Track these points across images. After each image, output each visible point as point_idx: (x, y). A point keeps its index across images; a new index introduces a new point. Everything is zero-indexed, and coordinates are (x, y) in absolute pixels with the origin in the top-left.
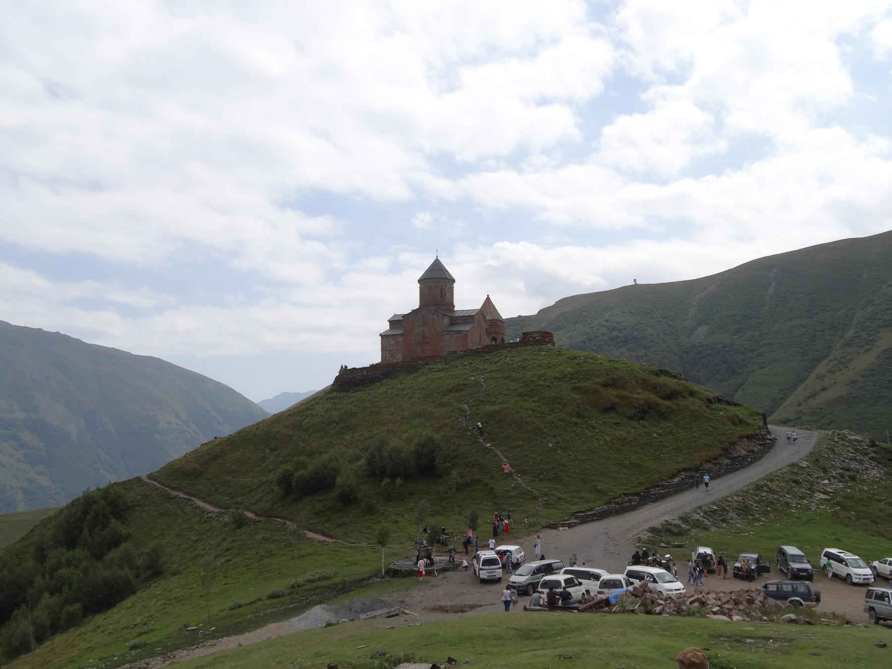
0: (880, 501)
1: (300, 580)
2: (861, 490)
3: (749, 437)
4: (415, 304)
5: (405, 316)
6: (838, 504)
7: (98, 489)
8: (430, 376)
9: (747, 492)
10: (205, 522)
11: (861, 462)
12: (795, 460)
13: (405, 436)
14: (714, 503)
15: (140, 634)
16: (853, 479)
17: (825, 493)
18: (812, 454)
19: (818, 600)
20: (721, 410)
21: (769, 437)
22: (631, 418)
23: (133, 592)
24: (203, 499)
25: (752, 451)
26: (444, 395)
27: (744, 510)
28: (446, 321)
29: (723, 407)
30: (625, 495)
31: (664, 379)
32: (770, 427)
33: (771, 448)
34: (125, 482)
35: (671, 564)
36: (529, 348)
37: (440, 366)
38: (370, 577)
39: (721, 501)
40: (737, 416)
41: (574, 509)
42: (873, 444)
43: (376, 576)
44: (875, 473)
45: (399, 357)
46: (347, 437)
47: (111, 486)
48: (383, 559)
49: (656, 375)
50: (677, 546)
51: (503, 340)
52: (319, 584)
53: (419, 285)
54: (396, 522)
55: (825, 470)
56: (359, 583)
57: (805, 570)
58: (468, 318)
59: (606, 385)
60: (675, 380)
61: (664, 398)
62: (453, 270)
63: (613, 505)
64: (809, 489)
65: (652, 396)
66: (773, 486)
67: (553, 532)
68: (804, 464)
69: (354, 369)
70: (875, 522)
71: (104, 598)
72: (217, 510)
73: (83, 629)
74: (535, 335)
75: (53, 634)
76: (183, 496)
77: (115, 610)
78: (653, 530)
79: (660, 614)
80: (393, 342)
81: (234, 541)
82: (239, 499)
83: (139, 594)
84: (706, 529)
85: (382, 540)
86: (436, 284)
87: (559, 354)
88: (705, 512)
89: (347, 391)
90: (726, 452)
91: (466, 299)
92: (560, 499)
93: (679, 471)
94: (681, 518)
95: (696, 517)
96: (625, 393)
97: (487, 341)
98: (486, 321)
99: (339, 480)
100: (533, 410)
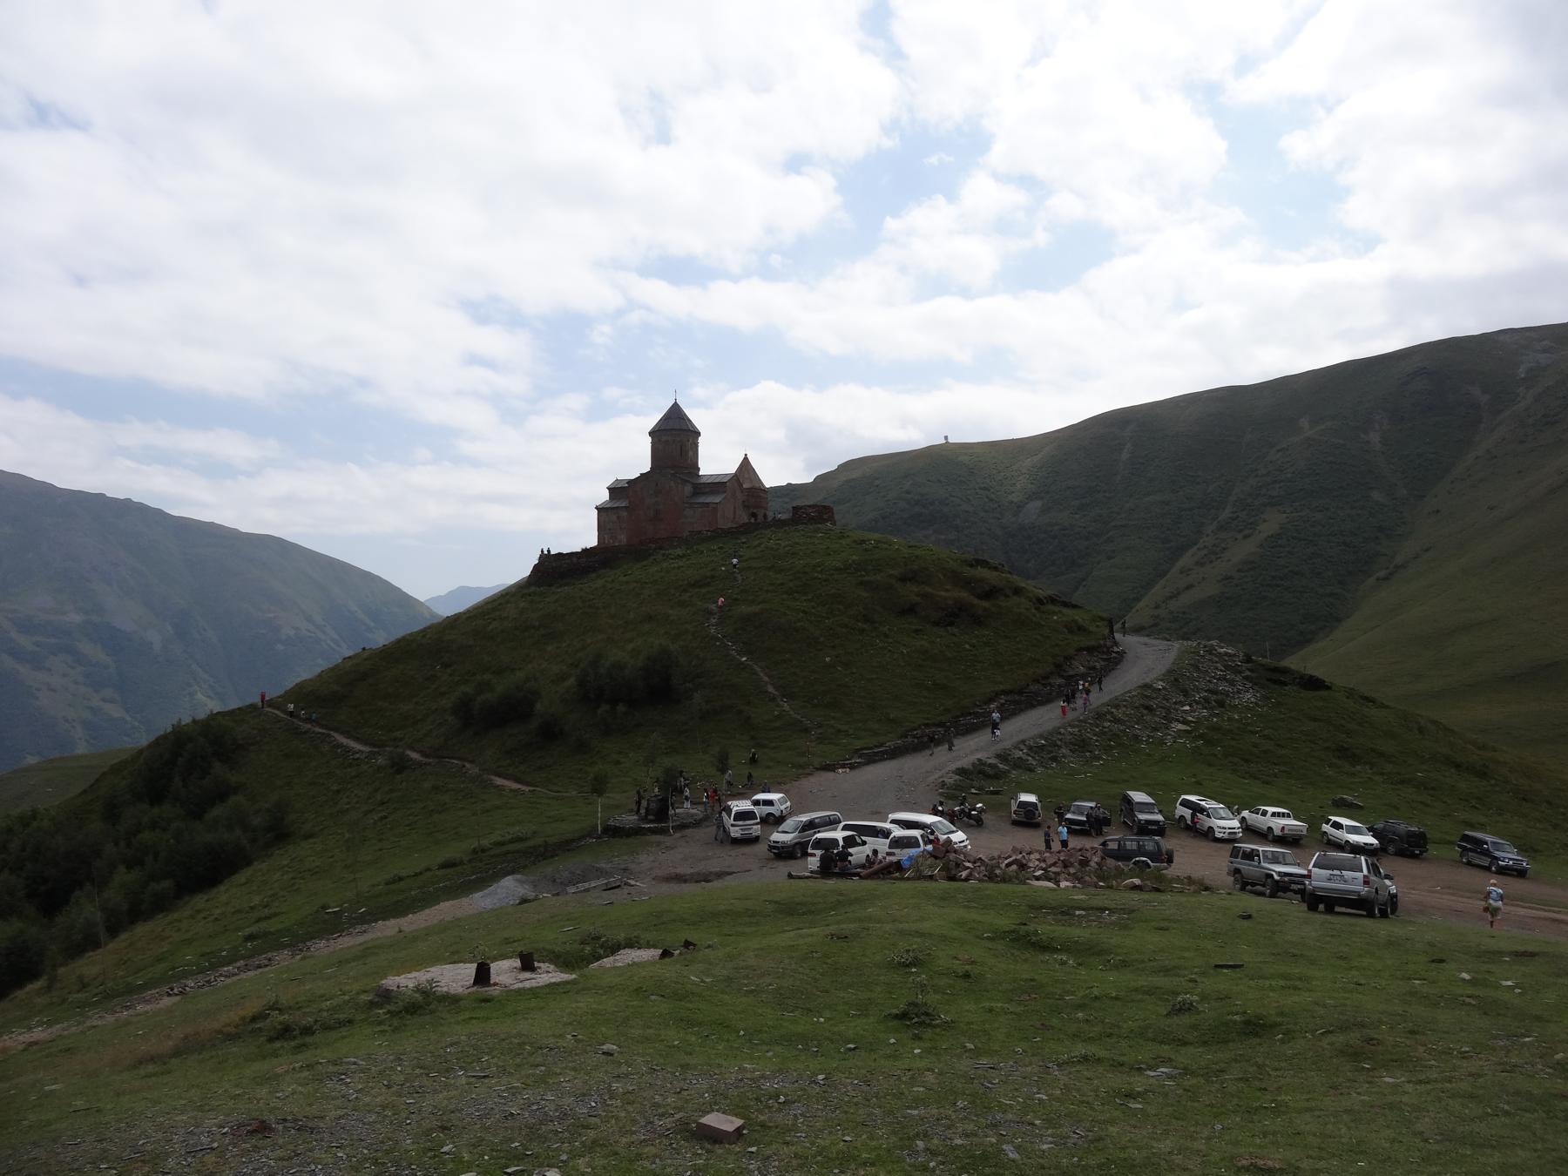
0: (1254, 733)
1: (485, 842)
2: (1230, 719)
3: (1090, 650)
4: (645, 465)
5: (630, 482)
6: (1201, 737)
7: (194, 721)
8: (665, 565)
10: (350, 765)
11: (1232, 683)
12: (1148, 680)
13: (630, 647)
14: (1041, 736)
15: (259, 920)
16: (1221, 704)
17: (1185, 722)
18: (1170, 672)
19: (1170, 860)
20: (1054, 613)
22: (936, 624)
23: (249, 863)
24: (348, 735)
25: (1094, 668)
26: (685, 591)
27: (1080, 745)
28: (688, 489)
29: (1056, 609)
30: (927, 725)
31: (981, 572)
32: (1118, 636)
33: (1117, 664)
34: (232, 712)
35: (984, 816)
36: (801, 527)
37: (679, 552)
40: (1075, 621)
41: (858, 744)
42: (1248, 660)
43: (590, 835)
44: (1249, 696)
45: (623, 539)
47: (213, 716)
48: (599, 812)
50: (993, 793)
51: (765, 516)
52: (511, 847)
54: (618, 763)
55: (1185, 693)
56: (568, 846)
57: (1156, 822)
58: (718, 485)
59: (903, 579)
60: (995, 573)
61: (980, 597)
62: (696, 416)
63: (910, 739)
65: (964, 595)
66: (1119, 714)
67: (830, 775)
68: (1160, 685)
69: (560, 554)
70: (1247, 761)
71: (206, 871)
72: (366, 749)
73: (176, 916)
74: (809, 509)
75: (132, 923)
77: (222, 888)
78: (961, 771)
79: (966, 880)
80: (614, 518)
82: (398, 734)
83: (257, 865)
84: (1031, 770)
85: (599, 786)
86: (675, 437)
88: (1030, 748)
89: (550, 585)
90: (1059, 668)
91: (715, 460)
94: (998, 756)
95: (1019, 754)
96: (929, 590)
97: (744, 518)
98: (742, 490)
99: (539, 707)
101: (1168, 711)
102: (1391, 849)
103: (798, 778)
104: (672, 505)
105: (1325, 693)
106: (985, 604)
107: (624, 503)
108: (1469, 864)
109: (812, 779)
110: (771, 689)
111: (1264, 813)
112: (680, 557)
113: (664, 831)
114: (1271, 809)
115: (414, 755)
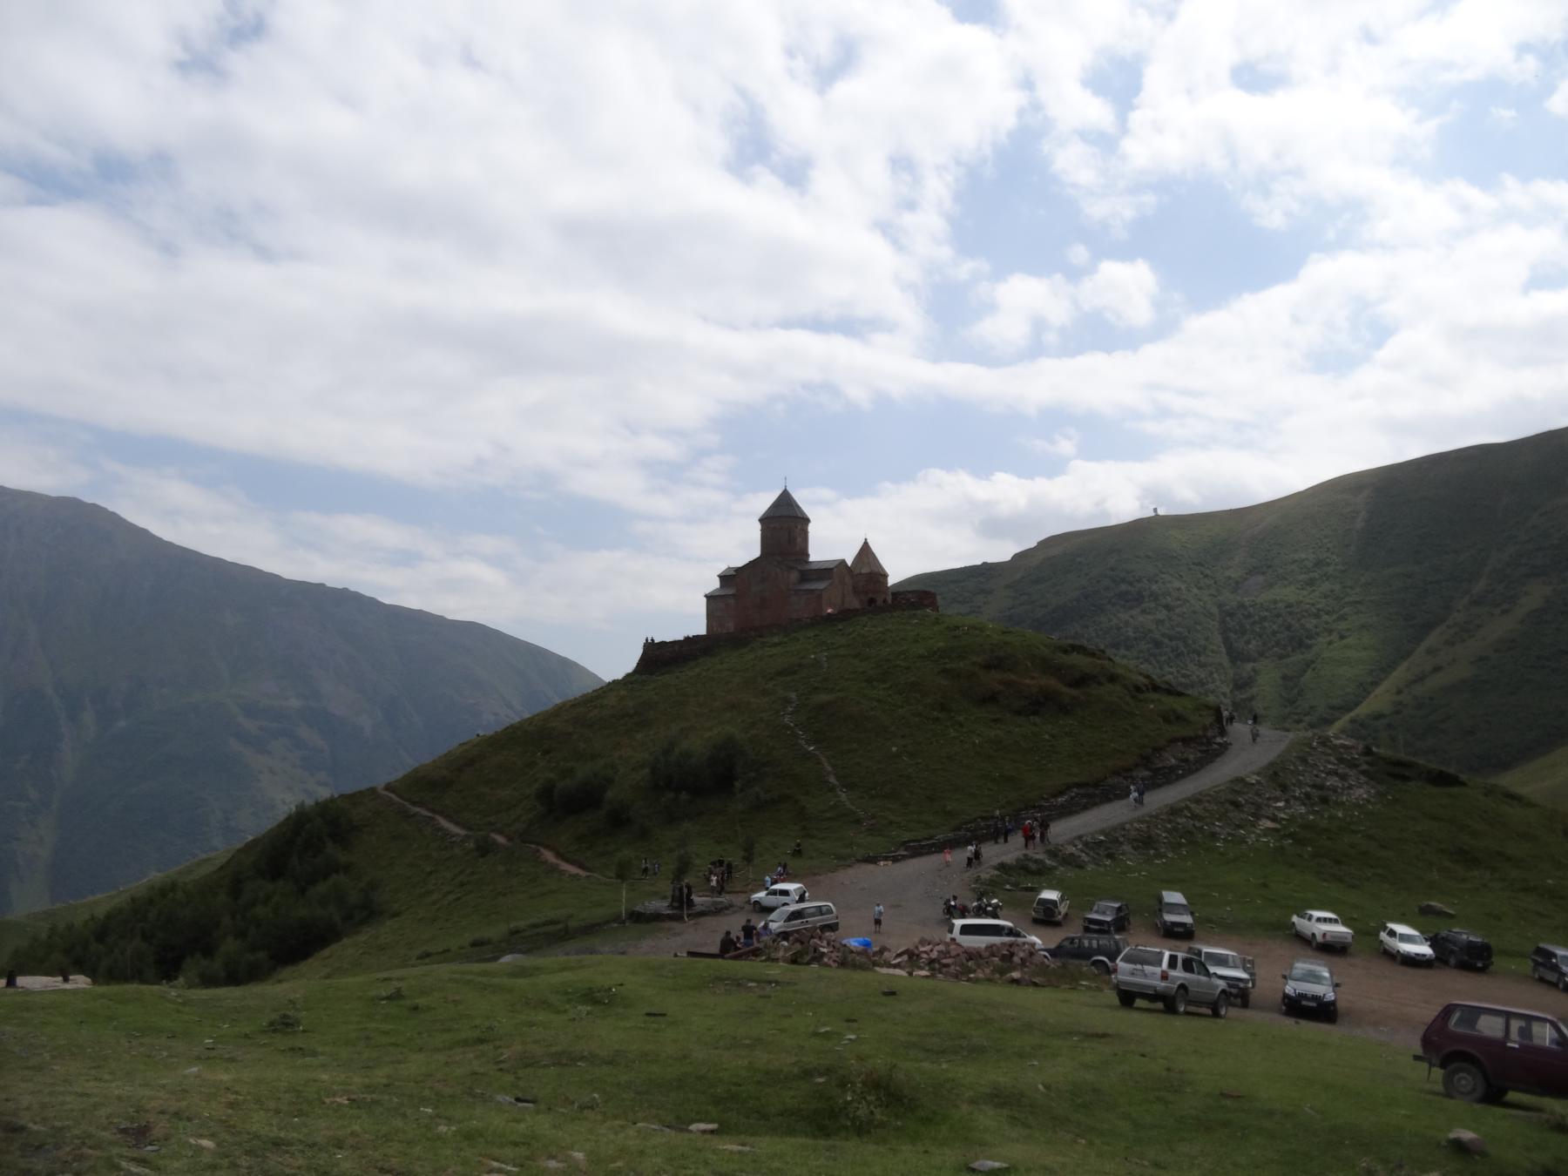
1: (521, 924)
2: (1331, 817)
3: (1186, 741)
4: (756, 552)
6: (1290, 835)
9: (1156, 817)
11: (1343, 777)
14: (1102, 832)
16: (1324, 800)
17: (1274, 819)
18: (1272, 764)
21: (1219, 740)
22: (1019, 713)
24: (449, 818)
25: (1186, 760)
28: (794, 576)
30: (983, 818)
33: (1218, 755)
37: (776, 639)
38: (607, 922)
39: (1115, 829)
41: (906, 836)
42: (1368, 752)
43: (615, 921)
44: (1361, 793)
45: (730, 626)
46: (639, 736)
48: (623, 899)
49: (1066, 652)
53: (759, 526)
55: (1284, 788)
56: (590, 929)
59: (988, 667)
61: (1070, 685)
63: (962, 833)
64: (1253, 815)
65: (1053, 683)
67: (871, 867)
68: (1253, 779)
72: (462, 832)
76: (425, 812)
79: (808, 963)
81: (473, 873)
83: (345, 941)
84: (1081, 867)
86: (785, 525)
87: (937, 622)
88: (1086, 844)
90: (1146, 761)
91: (829, 542)
92: (891, 823)
93: (1069, 787)
95: (1072, 849)
96: (1012, 677)
97: (854, 603)
99: (610, 794)
100: (879, 701)
101: (1259, 807)
102: (1452, 961)
103: (834, 869)
104: (784, 592)
105: (1455, 790)
106: (1074, 692)
107: (736, 593)
108: (1542, 980)
109: (850, 871)
110: (832, 779)
111: (1310, 918)
112: (776, 645)
113: (679, 918)
114: (1317, 914)
115: (500, 839)
